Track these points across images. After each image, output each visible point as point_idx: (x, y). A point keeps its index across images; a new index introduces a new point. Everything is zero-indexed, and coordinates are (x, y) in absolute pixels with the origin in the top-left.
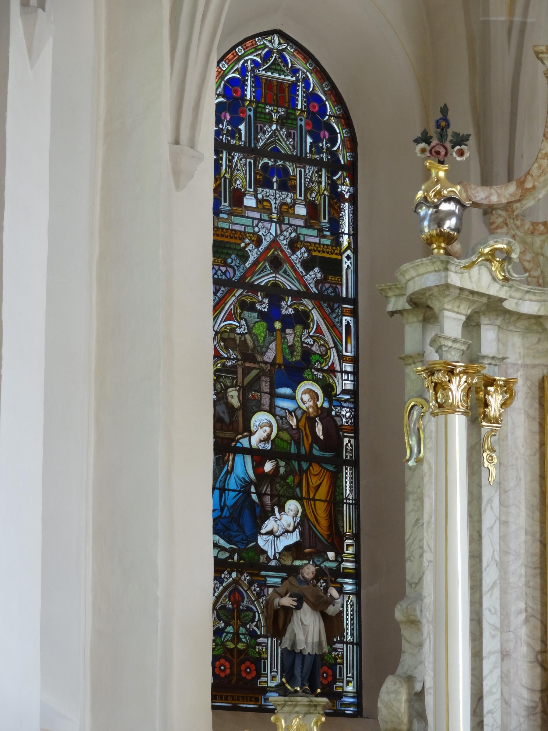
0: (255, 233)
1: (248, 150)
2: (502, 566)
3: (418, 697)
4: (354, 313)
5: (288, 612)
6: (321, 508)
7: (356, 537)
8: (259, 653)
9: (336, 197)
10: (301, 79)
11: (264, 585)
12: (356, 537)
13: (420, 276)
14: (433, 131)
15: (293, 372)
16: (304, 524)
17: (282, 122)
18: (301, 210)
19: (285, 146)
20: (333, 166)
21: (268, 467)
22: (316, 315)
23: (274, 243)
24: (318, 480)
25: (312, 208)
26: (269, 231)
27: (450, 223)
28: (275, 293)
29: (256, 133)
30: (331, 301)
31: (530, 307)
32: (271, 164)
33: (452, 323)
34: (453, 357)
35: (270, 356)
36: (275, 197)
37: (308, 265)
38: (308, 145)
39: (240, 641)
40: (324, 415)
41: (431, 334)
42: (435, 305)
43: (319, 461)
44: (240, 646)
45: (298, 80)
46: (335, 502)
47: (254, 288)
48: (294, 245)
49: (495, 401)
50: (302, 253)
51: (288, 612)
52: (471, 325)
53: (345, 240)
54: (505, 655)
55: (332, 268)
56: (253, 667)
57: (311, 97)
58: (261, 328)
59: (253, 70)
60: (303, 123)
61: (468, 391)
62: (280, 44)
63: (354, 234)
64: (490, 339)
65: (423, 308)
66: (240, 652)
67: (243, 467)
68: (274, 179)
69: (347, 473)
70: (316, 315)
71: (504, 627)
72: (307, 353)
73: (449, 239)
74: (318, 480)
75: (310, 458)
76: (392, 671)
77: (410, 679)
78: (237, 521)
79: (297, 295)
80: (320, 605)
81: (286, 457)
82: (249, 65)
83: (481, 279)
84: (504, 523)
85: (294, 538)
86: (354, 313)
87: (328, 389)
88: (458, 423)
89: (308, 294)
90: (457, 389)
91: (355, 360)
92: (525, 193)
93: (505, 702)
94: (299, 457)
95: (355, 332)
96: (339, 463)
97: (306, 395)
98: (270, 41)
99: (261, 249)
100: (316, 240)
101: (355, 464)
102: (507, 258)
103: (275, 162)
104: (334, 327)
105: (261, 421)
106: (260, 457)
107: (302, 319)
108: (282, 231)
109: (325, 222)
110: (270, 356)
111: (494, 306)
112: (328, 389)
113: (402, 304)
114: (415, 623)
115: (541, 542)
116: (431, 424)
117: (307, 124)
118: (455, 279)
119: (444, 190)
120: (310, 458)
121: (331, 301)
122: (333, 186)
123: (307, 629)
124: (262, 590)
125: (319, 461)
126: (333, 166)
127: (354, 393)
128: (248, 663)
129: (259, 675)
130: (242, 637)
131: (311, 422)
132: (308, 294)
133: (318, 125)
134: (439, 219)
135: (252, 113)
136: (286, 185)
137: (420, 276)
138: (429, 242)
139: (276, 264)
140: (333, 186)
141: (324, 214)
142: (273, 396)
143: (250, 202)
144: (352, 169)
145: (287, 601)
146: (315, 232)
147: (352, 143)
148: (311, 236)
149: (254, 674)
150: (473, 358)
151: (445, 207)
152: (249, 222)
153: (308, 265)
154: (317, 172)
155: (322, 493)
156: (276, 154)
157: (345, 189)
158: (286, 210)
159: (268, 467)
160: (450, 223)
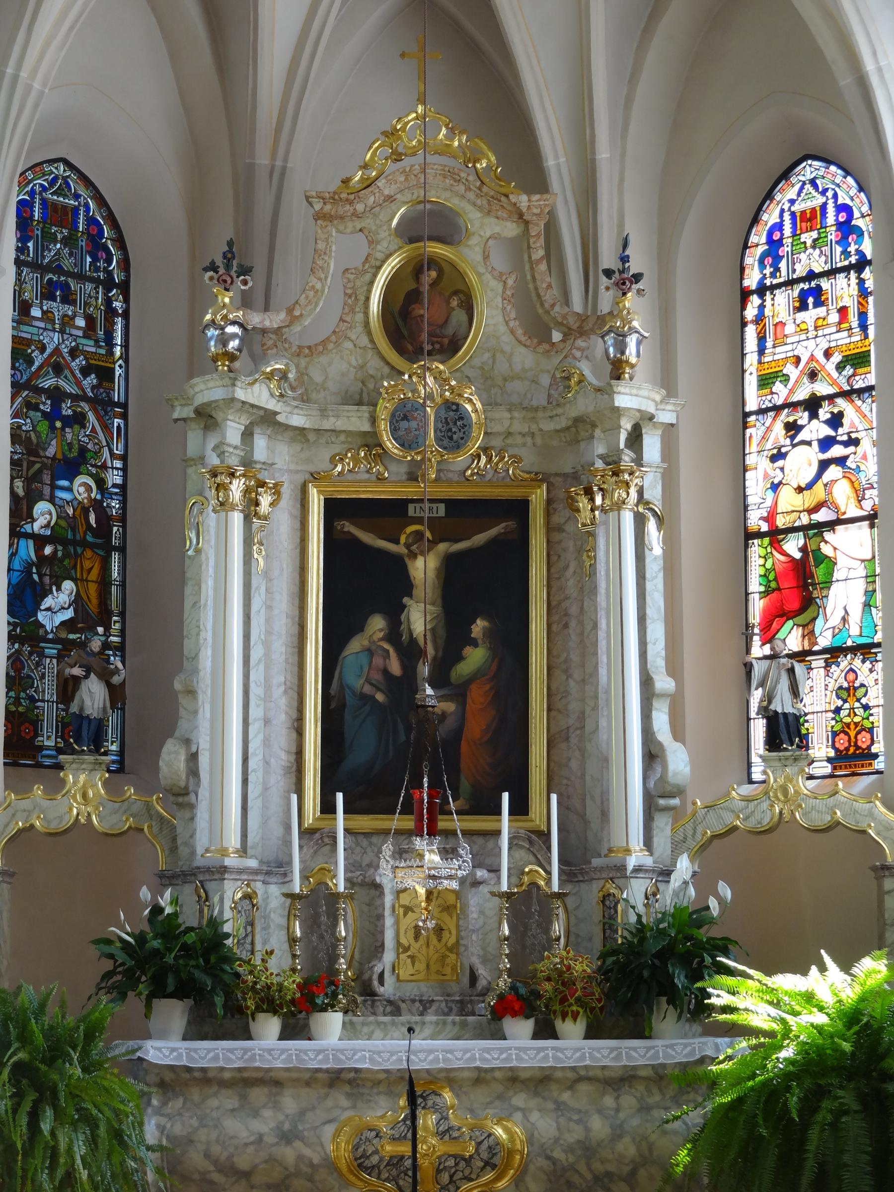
0: (40, 341)
1: (35, 266)
2: (267, 645)
3: (193, 757)
4: (124, 416)
5: (77, 680)
6: (93, 588)
7: (122, 615)
8: (37, 716)
9: (111, 312)
10: (82, 204)
11: (42, 655)
12: (122, 615)
13: (208, 390)
14: (219, 261)
15: (70, 467)
16: (78, 602)
17: (66, 241)
18: (81, 322)
19: (68, 264)
20: (109, 284)
21: (48, 550)
22: (91, 416)
23: (57, 351)
24: (90, 562)
25: (90, 320)
26: (53, 340)
27: (233, 344)
28: (57, 395)
29: (43, 251)
30: (104, 405)
31: (297, 420)
32: (55, 279)
33: (233, 432)
34: (233, 461)
35: (51, 451)
36: (58, 309)
37: (86, 371)
38: (88, 264)
39: (20, 704)
40: (97, 505)
41: (211, 443)
42: (219, 415)
43: (91, 546)
44: (21, 709)
45: (79, 203)
46: (104, 582)
47: (38, 391)
48: (74, 353)
49: (265, 501)
50: (80, 361)
51: (77, 680)
52: (248, 435)
53: (118, 351)
54: (267, 721)
55: (106, 375)
56: (31, 728)
57: (91, 221)
58: (43, 427)
59: (40, 193)
60: (84, 244)
61: (247, 491)
62: (64, 171)
63: (126, 346)
64: (261, 446)
65: (207, 418)
66: (20, 714)
67: (27, 549)
68: (58, 293)
69: (115, 557)
70: (91, 416)
71: (267, 698)
72: (83, 450)
73: (232, 357)
74: (90, 562)
75: (85, 544)
76: (171, 735)
77: (187, 742)
78: (25, 596)
79: (75, 398)
80: (106, 676)
81: (64, 542)
82: (37, 188)
83: (260, 395)
84: (269, 608)
85: (69, 614)
86: (124, 416)
87: (101, 483)
88: (237, 519)
89: (85, 398)
90: (237, 488)
91: (124, 458)
92: (293, 319)
93: (267, 763)
94: (74, 542)
95: (124, 433)
96: (109, 549)
97: (82, 487)
98: (56, 168)
99: (45, 355)
100: (93, 350)
101: (122, 550)
102: (284, 376)
103: (59, 278)
104: (107, 428)
105: (42, 508)
106: (40, 541)
107: (79, 419)
108: (63, 340)
109: (101, 334)
110: (51, 451)
111: (268, 419)
112: (101, 483)
113: (187, 412)
114: (191, 692)
115: (299, 625)
116: (211, 519)
117: (87, 245)
118: (240, 394)
119: (227, 315)
120: (85, 544)
121: (104, 405)
122: (108, 301)
123: (93, 696)
124: (40, 660)
125: (91, 546)
126: (109, 284)
127: (123, 487)
128: (27, 725)
129: (36, 735)
130: (22, 701)
131: (85, 511)
132: (85, 398)
133: (96, 246)
134: (224, 340)
135: (39, 233)
136: (67, 299)
137: (208, 390)
138: (215, 359)
139: (58, 369)
140: (108, 301)
141: (99, 326)
142: (53, 487)
143: (36, 312)
144: (125, 288)
145: (77, 671)
146: (92, 343)
147: (125, 264)
148: (89, 346)
149: (32, 734)
150: (248, 462)
151: (230, 329)
152: (35, 331)
153: (86, 371)
154: (95, 289)
155: (94, 575)
156: (59, 270)
157: (118, 305)
158: (67, 322)
159: (48, 550)
160: (233, 344)
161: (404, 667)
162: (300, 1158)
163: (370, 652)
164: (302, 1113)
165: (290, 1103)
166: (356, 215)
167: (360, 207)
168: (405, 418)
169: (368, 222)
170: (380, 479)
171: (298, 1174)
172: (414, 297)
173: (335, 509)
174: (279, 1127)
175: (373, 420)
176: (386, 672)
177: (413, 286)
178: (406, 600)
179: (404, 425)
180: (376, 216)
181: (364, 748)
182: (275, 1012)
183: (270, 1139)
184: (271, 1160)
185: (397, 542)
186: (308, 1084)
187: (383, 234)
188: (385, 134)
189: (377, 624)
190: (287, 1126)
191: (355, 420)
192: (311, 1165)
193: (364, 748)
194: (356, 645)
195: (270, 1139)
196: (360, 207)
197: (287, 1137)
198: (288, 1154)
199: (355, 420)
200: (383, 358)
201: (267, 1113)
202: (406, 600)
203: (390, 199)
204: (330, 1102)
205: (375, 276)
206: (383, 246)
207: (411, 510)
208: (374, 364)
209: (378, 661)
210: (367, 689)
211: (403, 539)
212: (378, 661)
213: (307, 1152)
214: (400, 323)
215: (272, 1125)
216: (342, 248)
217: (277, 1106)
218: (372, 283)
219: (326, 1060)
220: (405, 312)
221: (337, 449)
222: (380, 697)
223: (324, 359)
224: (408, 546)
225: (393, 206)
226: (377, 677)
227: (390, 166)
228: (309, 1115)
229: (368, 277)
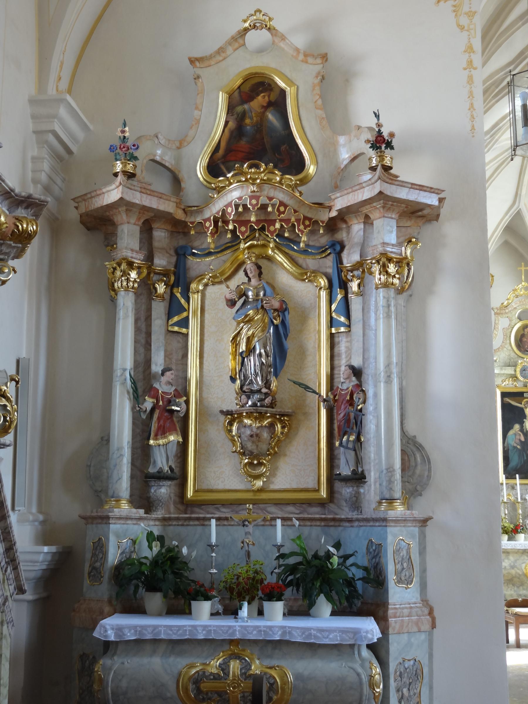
161: (525, 439)
162: (516, 572)
163: (515, 434)
164: (516, 561)
165: (512, 558)
166: (506, 313)
167: (507, 311)
168: (524, 370)
169: (509, 315)
170: (516, 386)
171: (515, 577)
172: (523, 336)
173: (504, 395)
174: (510, 564)
175: (515, 371)
176: (520, 440)
177: (522, 332)
178: (524, 420)
179: (524, 372)
180: (511, 313)
181: (515, 461)
182: (507, 533)
183: (508, 567)
184: (509, 573)
185: (521, 404)
186: (516, 553)
187: (514, 318)
188: (513, 290)
189: (517, 427)
190: (512, 564)
191: (510, 371)
192: (519, 574)
193: (515, 461)
194: (511, 433)
195: (508, 567)
196: (507, 311)
197: (512, 567)
198: (513, 572)
199: (510, 371)
200: (515, 353)
201: (506, 561)
202: (524, 420)
203: (515, 308)
204: (522, 558)
205: (512, 330)
206: (514, 322)
207: (525, 395)
208: (513, 355)
209: (518, 437)
210: (515, 445)
211: (523, 403)
212: (518, 437)
213: (518, 571)
214: (520, 343)
215: (508, 564)
216: (503, 323)
217: (508, 559)
218: (511, 332)
219: (522, 546)
220: (521, 340)
221: (503, 378)
222: (519, 447)
223: (498, 353)
224: (524, 405)
225: (516, 310)
226: (518, 441)
227: (516, 300)
228: (518, 561)
229: (510, 330)
